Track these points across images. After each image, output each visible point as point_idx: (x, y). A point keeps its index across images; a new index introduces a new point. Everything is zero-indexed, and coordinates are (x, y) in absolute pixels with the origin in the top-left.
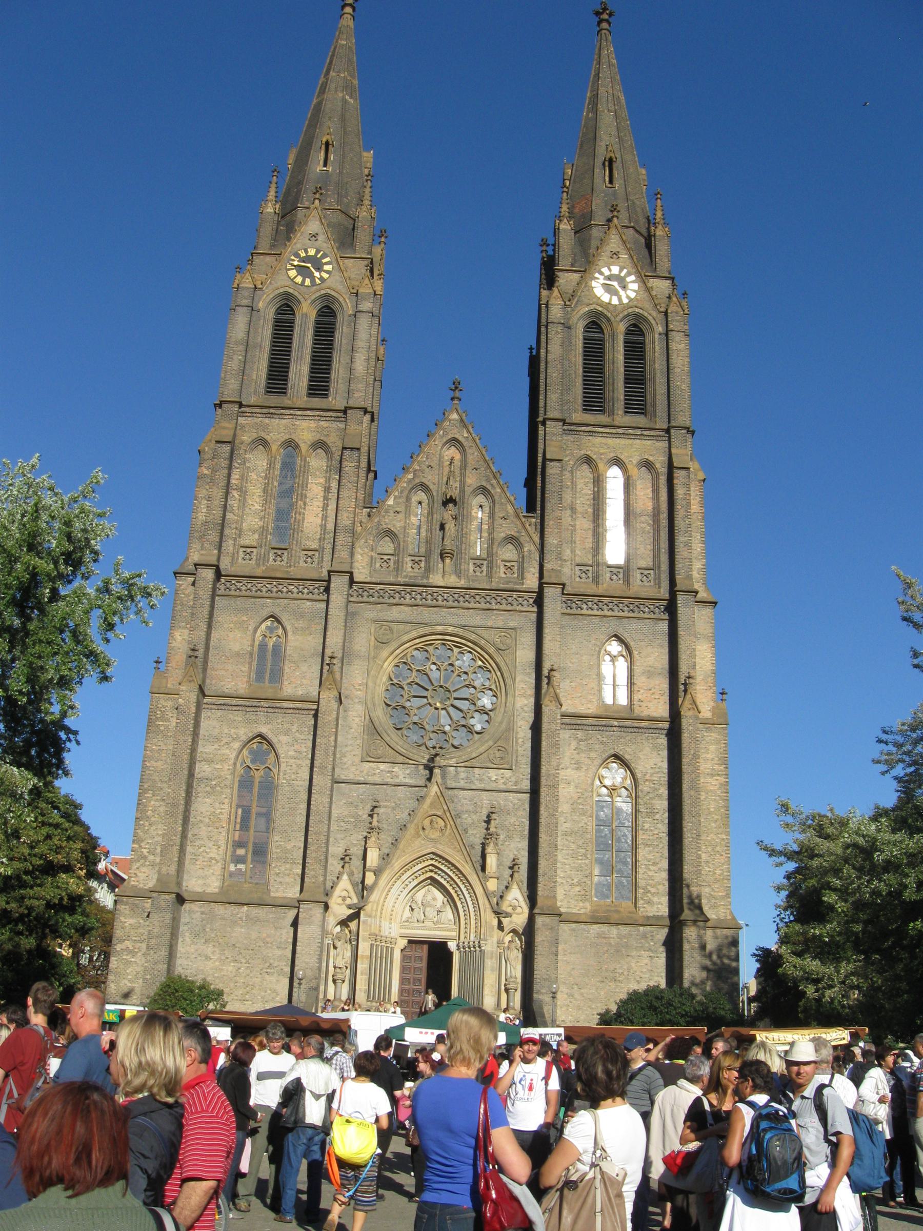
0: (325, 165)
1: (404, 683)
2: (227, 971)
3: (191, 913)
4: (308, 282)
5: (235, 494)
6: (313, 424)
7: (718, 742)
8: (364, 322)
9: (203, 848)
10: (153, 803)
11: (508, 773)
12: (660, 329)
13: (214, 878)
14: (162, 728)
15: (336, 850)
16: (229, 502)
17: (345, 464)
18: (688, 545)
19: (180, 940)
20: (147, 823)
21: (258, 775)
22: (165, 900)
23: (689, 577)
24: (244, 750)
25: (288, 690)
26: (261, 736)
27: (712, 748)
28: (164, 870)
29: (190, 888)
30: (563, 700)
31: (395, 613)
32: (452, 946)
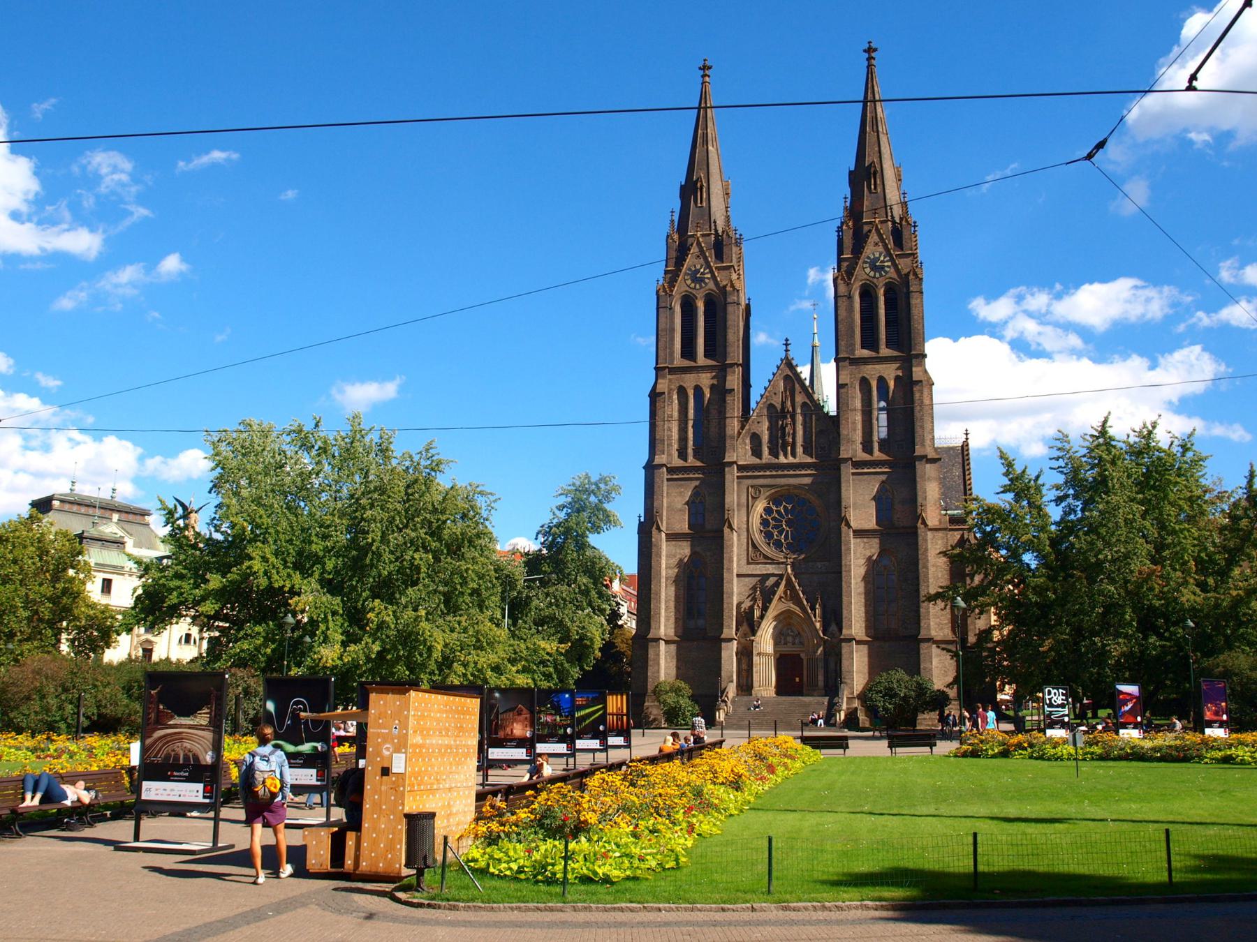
0: (701, 202)
1: (770, 518)
4: (698, 286)
6: (709, 375)
7: (943, 538)
8: (730, 309)
11: (827, 563)
12: (905, 290)
17: (728, 398)
18: (922, 427)
23: (923, 445)
25: (708, 527)
27: (940, 542)
30: (852, 524)
31: (761, 481)
32: (803, 655)
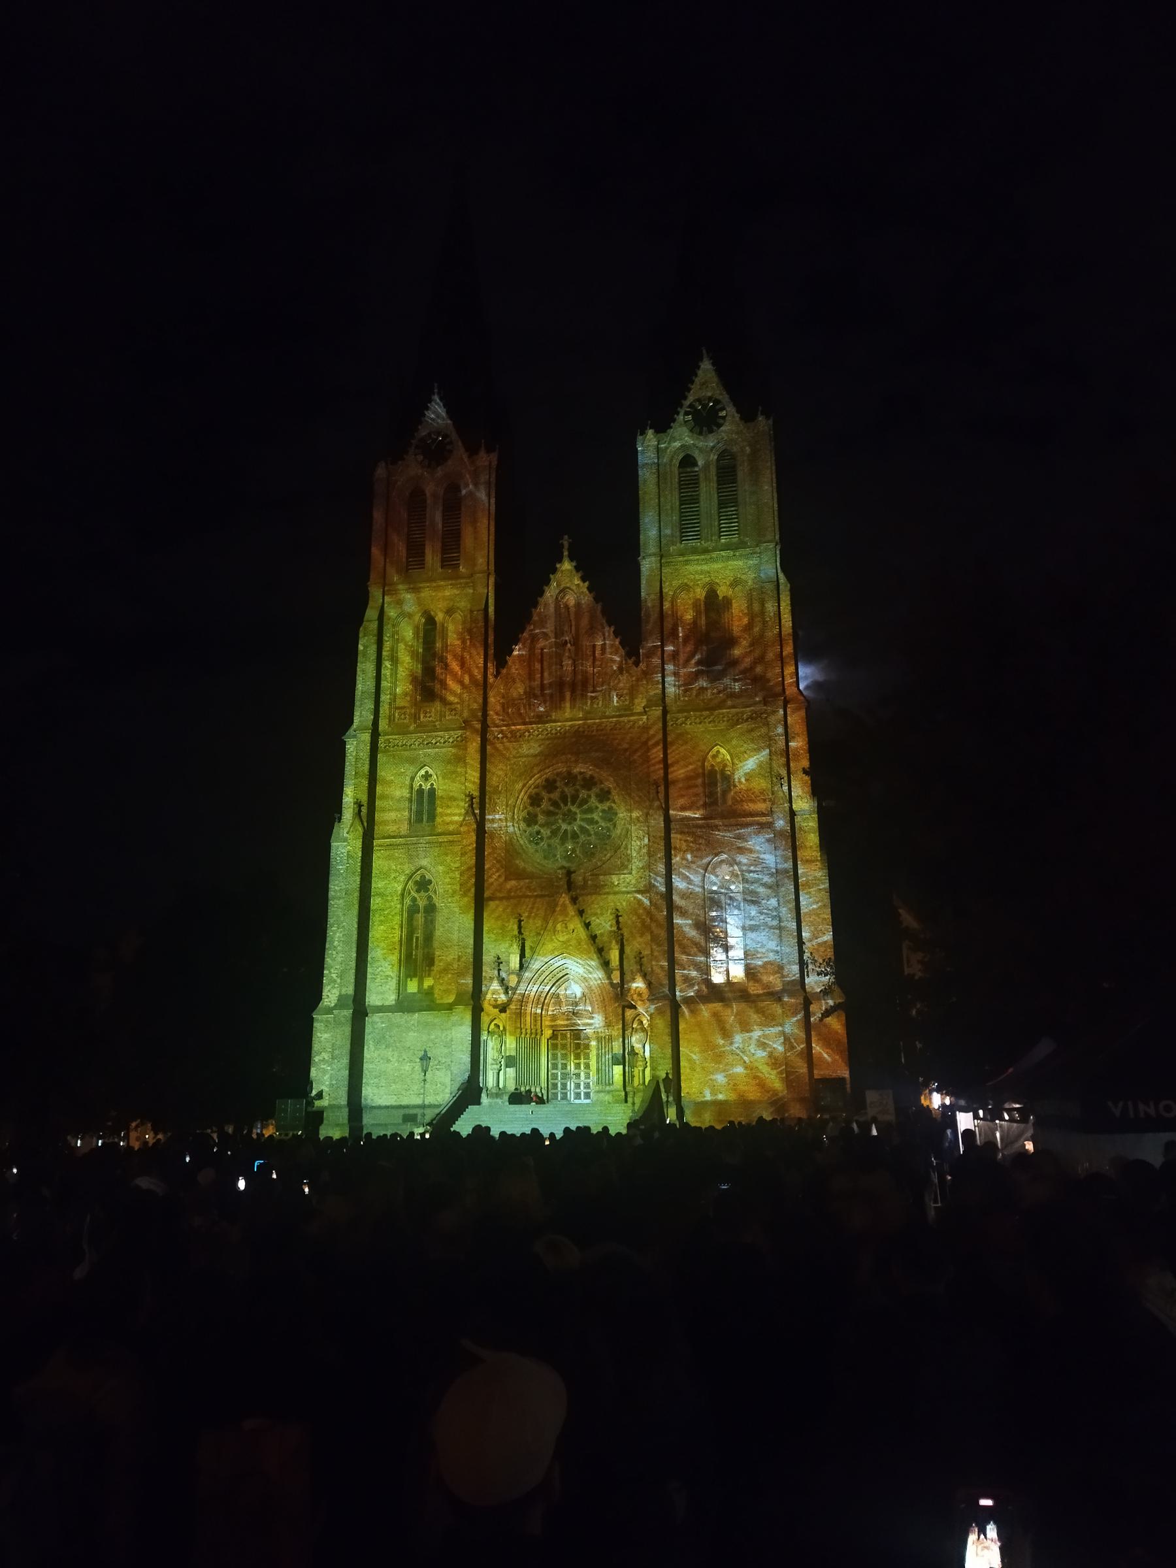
2: (405, 1070)
3: (374, 1024)
5: (387, 664)
9: (380, 969)
10: (338, 934)
13: (391, 992)
14: (342, 871)
15: (488, 957)
16: (383, 672)
19: (366, 1047)
20: (334, 953)
21: (422, 903)
22: (344, 1016)
24: (410, 882)
26: (421, 868)
28: (343, 992)
29: (372, 1003)
